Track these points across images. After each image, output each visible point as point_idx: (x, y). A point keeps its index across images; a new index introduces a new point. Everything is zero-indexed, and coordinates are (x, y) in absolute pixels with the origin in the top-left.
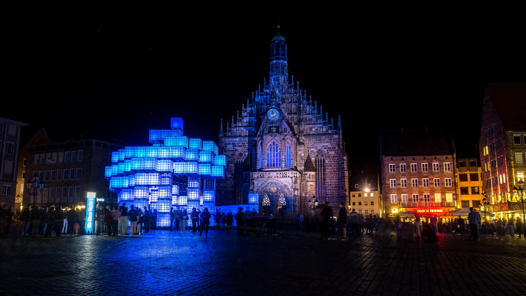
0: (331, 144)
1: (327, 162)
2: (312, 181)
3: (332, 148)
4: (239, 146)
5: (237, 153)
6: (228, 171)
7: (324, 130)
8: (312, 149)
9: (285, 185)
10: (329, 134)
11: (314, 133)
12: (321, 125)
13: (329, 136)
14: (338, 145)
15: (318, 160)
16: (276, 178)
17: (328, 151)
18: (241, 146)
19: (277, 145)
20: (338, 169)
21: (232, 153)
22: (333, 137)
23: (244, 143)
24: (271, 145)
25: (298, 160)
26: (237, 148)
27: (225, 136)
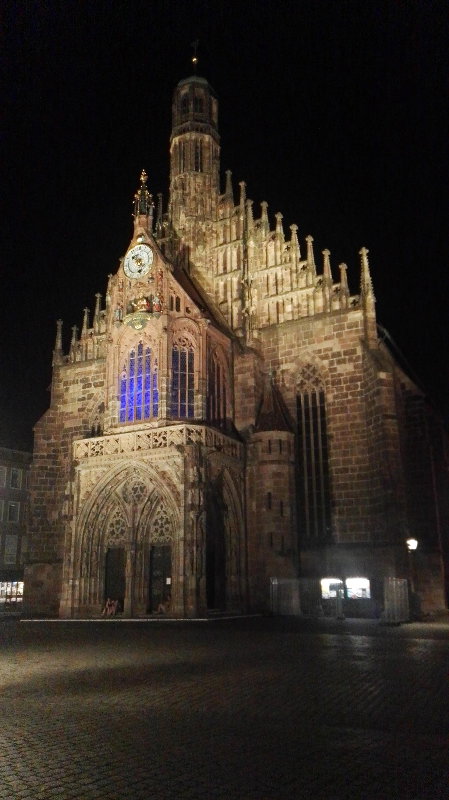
0: (342, 341)
1: (330, 398)
2: (278, 462)
3: (346, 353)
4: (96, 386)
7: (320, 303)
8: (284, 367)
9: (163, 474)
10: (336, 313)
11: (290, 318)
12: (310, 291)
13: (334, 318)
14: (364, 342)
15: (306, 397)
16: (136, 453)
17: (331, 363)
19: (148, 351)
21: (80, 405)
22: (345, 319)
24: (132, 355)
25: (238, 400)
26: (93, 390)
27: (67, 362)
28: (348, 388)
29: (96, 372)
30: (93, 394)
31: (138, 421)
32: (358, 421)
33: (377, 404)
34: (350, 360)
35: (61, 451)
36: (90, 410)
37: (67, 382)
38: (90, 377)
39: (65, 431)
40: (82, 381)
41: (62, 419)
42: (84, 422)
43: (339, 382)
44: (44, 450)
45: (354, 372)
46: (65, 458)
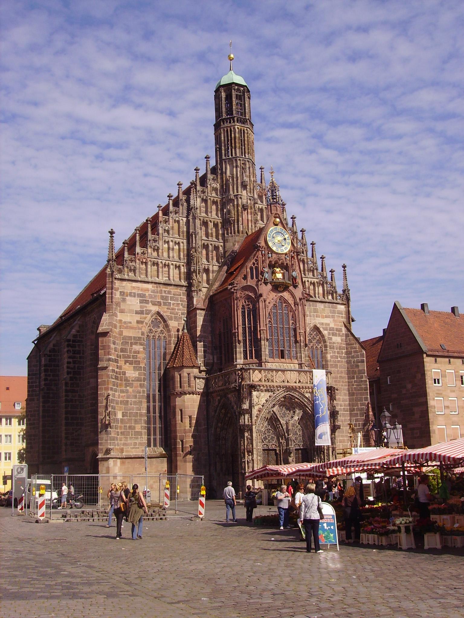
1: (329, 356)
3: (337, 330)
4: (154, 304)
5: (148, 318)
6: (131, 363)
13: (331, 305)
17: (329, 334)
18: (159, 304)
20: (348, 373)
21: (138, 317)
23: (166, 298)
28: (338, 353)
29: (153, 291)
30: (150, 311)
31: (283, 360)
32: (343, 375)
33: (360, 368)
34: (339, 335)
35: (120, 356)
36: (147, 324)
37: (124, 293)
38: (147, 294)
39: (125, 338)
40: (139, 295)
41: (120, 326)
42: (143, 334)
43: (333, 348)
44: (114, 354)
45: (341, 343)
46: (125, 364)
